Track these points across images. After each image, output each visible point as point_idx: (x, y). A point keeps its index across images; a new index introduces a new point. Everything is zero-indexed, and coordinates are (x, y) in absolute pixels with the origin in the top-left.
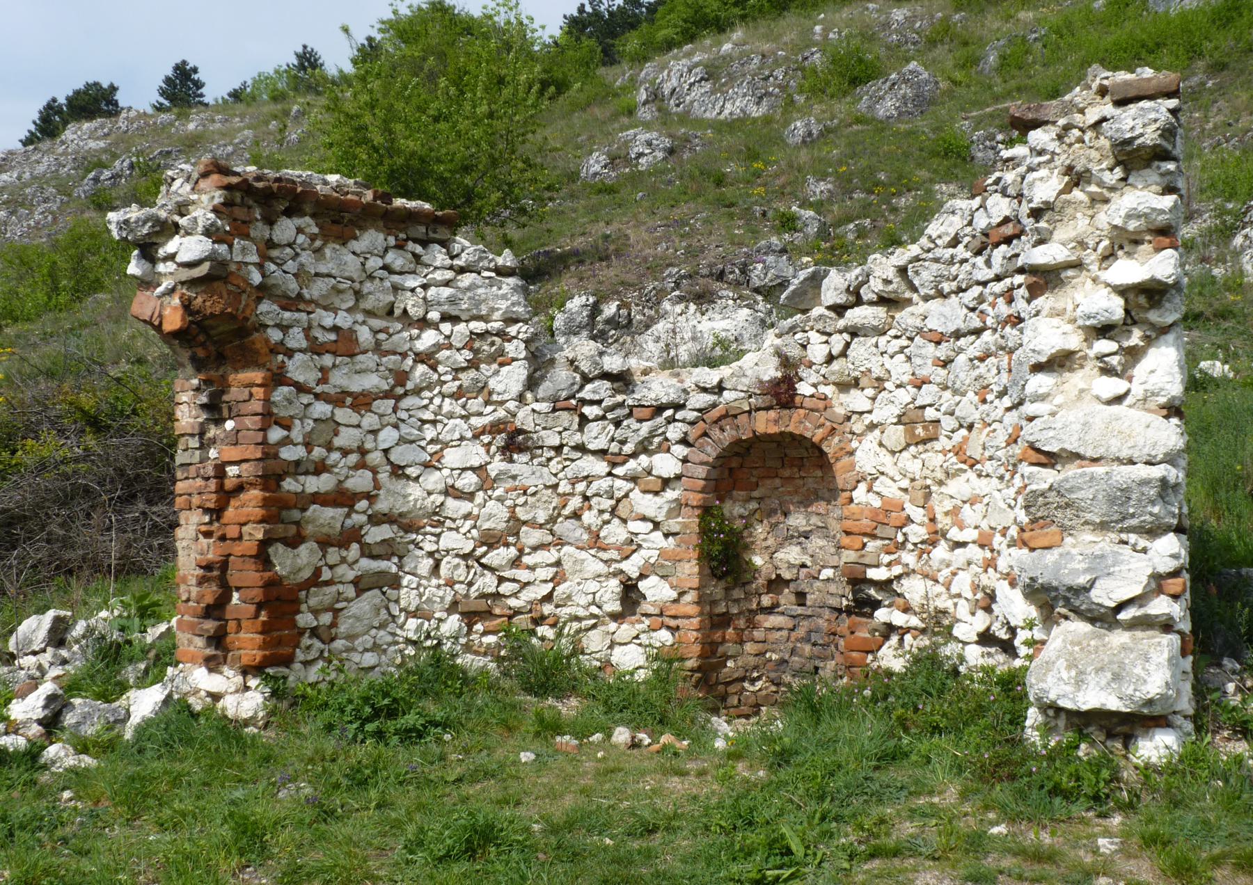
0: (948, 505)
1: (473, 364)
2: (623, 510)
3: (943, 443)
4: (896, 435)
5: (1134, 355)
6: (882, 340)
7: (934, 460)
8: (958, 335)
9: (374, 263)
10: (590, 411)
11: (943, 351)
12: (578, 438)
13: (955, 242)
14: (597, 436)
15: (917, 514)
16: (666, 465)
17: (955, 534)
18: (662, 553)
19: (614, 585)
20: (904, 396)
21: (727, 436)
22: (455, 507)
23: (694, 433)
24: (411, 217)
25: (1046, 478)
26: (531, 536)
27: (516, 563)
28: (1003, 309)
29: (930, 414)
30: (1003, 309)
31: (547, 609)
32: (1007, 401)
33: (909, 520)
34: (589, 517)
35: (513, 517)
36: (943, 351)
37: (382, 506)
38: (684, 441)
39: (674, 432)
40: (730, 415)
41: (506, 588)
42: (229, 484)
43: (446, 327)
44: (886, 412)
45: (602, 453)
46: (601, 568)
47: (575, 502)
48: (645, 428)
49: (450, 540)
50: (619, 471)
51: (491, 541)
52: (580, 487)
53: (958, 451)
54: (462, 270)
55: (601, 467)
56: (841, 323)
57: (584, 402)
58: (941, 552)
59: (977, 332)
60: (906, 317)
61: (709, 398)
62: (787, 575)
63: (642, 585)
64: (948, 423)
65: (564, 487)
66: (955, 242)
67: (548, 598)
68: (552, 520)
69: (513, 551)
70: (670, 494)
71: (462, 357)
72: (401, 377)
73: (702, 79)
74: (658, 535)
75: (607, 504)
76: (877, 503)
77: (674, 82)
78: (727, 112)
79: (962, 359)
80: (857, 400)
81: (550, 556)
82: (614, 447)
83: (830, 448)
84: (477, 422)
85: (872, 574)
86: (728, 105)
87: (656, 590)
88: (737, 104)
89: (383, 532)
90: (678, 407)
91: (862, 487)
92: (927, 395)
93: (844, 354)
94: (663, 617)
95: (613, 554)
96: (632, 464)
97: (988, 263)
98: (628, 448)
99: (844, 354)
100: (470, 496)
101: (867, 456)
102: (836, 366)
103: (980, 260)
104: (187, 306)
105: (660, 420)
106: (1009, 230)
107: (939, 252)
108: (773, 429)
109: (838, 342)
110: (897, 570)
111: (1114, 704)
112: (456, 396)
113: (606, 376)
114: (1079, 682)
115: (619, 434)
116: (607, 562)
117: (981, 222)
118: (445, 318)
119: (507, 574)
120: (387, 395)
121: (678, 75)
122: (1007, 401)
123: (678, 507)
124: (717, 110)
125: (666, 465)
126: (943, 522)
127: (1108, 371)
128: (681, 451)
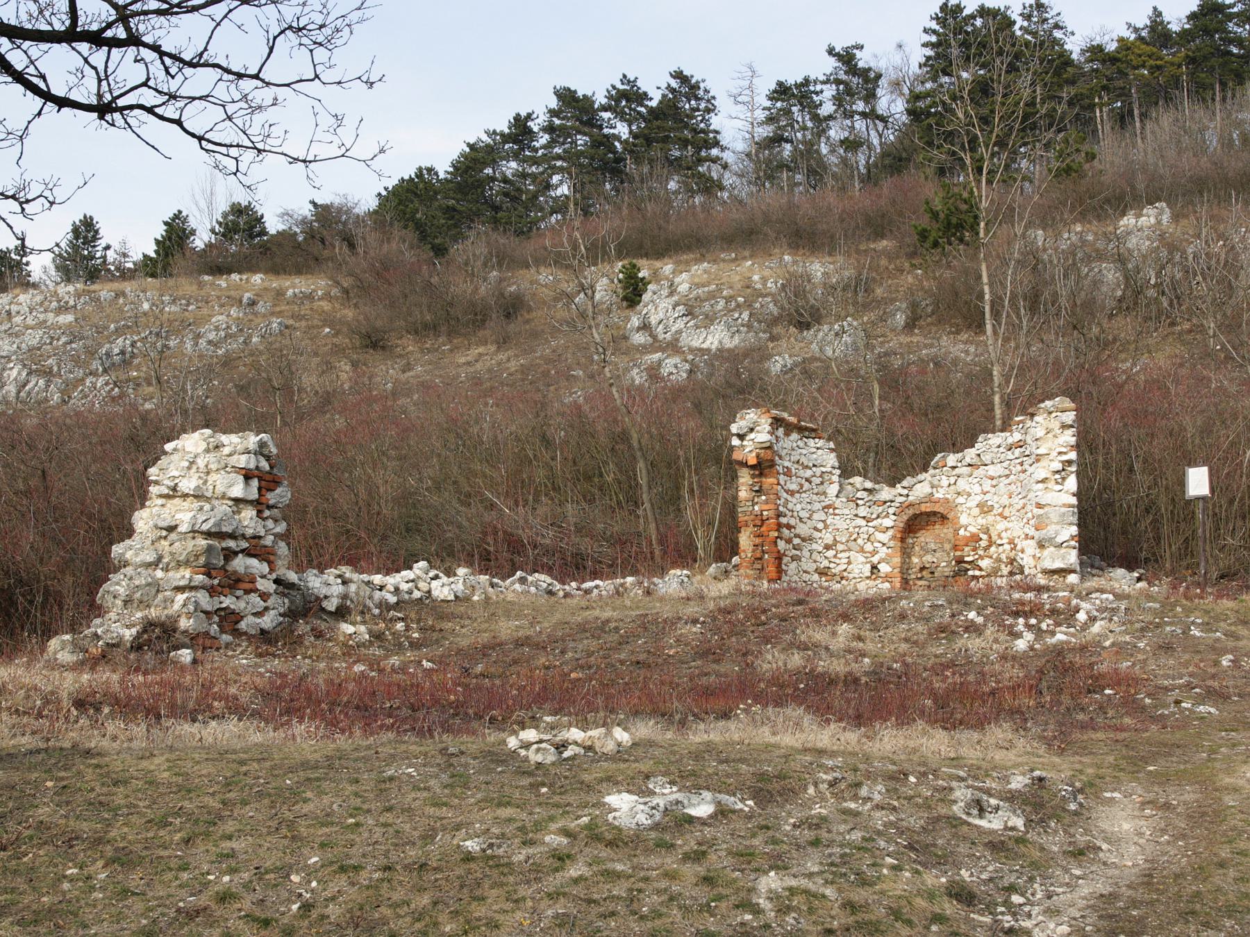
0: (996, 533)
1: (822, 483)
2: (872, 538)
3: (995, 512)
4: (976, 511)
5: (1064, 479)
6: (970, 479)
7: (990, 518)
8: (1000, 477)
9: (795, 445)
10: (860, 502)
11: (994, 482)
12: (856, 512)
13: (999, 446)
14: (863, 511)
15: (984, 537)
16: (888, 522)
17: (999, 542)
18: (887, 554)
19: (868, 566)
20: (979, 498)
21: (911, 512)
22: (817, 534)
23: (898, 511)
24: (806, 429)
25: (1041, 511)
26: (840, 547)
27: (835, 556)
28: (1019, 468)
29: (989, 503)
30: (1019, 468)
31: (845, 574)
32: (1020, 496)
33: (981, 539)
34: (860, 541)
35: (835, 539)
36: (994, 482)
37: (798, 531)
38: (894, 514)
39: (891, 511)
40: (911, 505)
41: (832, 565)
42: (764, 518)
43: (814, 469)
44: (973, 502)
45: (864, 518)
46: (864, 560)
47: (855, 536)
48: (881, 509)
49: (814, 546)
50: (870, 524)
51: (827, 547)
52: (857, 530)
53: (1001, 515)
54: (818, 448)
55: (863, 523)
56: (954, 473)
57: (858, 499)
58: (993, 549)
59: (1007, 476)
60: (981, 471)
61: (904, 499)
62: (927, 566)
63: (879, 566)
64: (996, 506)
65: (851, 530)
66: (999, 446)
67: (845, 570)
68: (848, 541)
69: (834, 552)
70: (890, 533)
71: (818, 480)
72: (802, 486)
73: (683, 315)
74: (885, 548)
75: (866, 537)
76: (968, 534)
77: (661, 315)
78: (708, 343)
79: (1001, 484)
80: (961, 500)
81: (847, 554)
82: (869, 515)
83: (950, 516)
84: (823, 504)
85: (967, 559)
86: (710, 337)
87: (884, 568)
88: (717, 336)
89: (796, 541)
90: (892, 501)
91: (962, 530)
92: (987, 497)
93: (955, 484)
94: (887, 578)
95: (869, 555)
96: (875, 522)
97: (1013, 453)
98: (874, 516)
99: (955, 484)
100: (820, 531)
101: (964, 519)
102: (952, 487)
103: (1009, 453)
104: (758, 456)
105: (886, 506)
106: (1021, 444)
107: (993, 449)
108: (928, 510)
109: (952, 480)
110: (977, 557)
111: (1062, 566)
112: (817, 494)
113: (865, 490)
114: (1053, 561)
115: (870, 510)
116: (866, 558)
117: (1010, 440)
118: (814, 466)
119: (833, 560)
120: (798, 492)
121: (664, 310)
122: (1020, 496)
123: (893, 538)
124: (701, 340)
125: (888, 522)
126: (994, 538)
127: (1057, 483)
128: (894, 518)
